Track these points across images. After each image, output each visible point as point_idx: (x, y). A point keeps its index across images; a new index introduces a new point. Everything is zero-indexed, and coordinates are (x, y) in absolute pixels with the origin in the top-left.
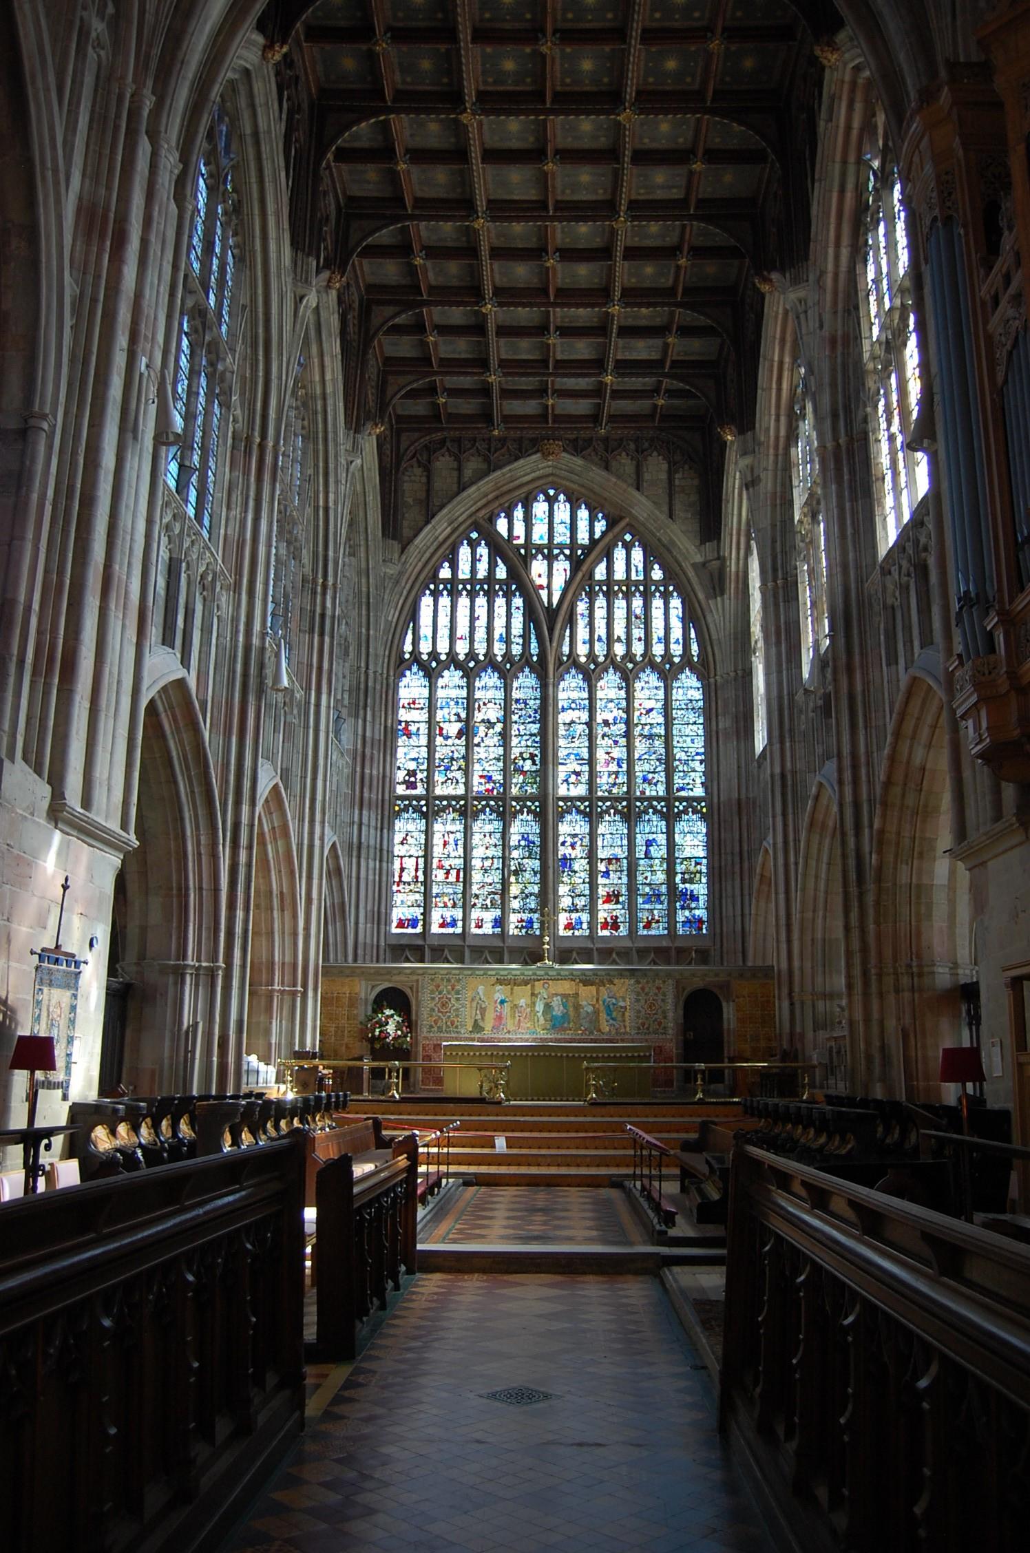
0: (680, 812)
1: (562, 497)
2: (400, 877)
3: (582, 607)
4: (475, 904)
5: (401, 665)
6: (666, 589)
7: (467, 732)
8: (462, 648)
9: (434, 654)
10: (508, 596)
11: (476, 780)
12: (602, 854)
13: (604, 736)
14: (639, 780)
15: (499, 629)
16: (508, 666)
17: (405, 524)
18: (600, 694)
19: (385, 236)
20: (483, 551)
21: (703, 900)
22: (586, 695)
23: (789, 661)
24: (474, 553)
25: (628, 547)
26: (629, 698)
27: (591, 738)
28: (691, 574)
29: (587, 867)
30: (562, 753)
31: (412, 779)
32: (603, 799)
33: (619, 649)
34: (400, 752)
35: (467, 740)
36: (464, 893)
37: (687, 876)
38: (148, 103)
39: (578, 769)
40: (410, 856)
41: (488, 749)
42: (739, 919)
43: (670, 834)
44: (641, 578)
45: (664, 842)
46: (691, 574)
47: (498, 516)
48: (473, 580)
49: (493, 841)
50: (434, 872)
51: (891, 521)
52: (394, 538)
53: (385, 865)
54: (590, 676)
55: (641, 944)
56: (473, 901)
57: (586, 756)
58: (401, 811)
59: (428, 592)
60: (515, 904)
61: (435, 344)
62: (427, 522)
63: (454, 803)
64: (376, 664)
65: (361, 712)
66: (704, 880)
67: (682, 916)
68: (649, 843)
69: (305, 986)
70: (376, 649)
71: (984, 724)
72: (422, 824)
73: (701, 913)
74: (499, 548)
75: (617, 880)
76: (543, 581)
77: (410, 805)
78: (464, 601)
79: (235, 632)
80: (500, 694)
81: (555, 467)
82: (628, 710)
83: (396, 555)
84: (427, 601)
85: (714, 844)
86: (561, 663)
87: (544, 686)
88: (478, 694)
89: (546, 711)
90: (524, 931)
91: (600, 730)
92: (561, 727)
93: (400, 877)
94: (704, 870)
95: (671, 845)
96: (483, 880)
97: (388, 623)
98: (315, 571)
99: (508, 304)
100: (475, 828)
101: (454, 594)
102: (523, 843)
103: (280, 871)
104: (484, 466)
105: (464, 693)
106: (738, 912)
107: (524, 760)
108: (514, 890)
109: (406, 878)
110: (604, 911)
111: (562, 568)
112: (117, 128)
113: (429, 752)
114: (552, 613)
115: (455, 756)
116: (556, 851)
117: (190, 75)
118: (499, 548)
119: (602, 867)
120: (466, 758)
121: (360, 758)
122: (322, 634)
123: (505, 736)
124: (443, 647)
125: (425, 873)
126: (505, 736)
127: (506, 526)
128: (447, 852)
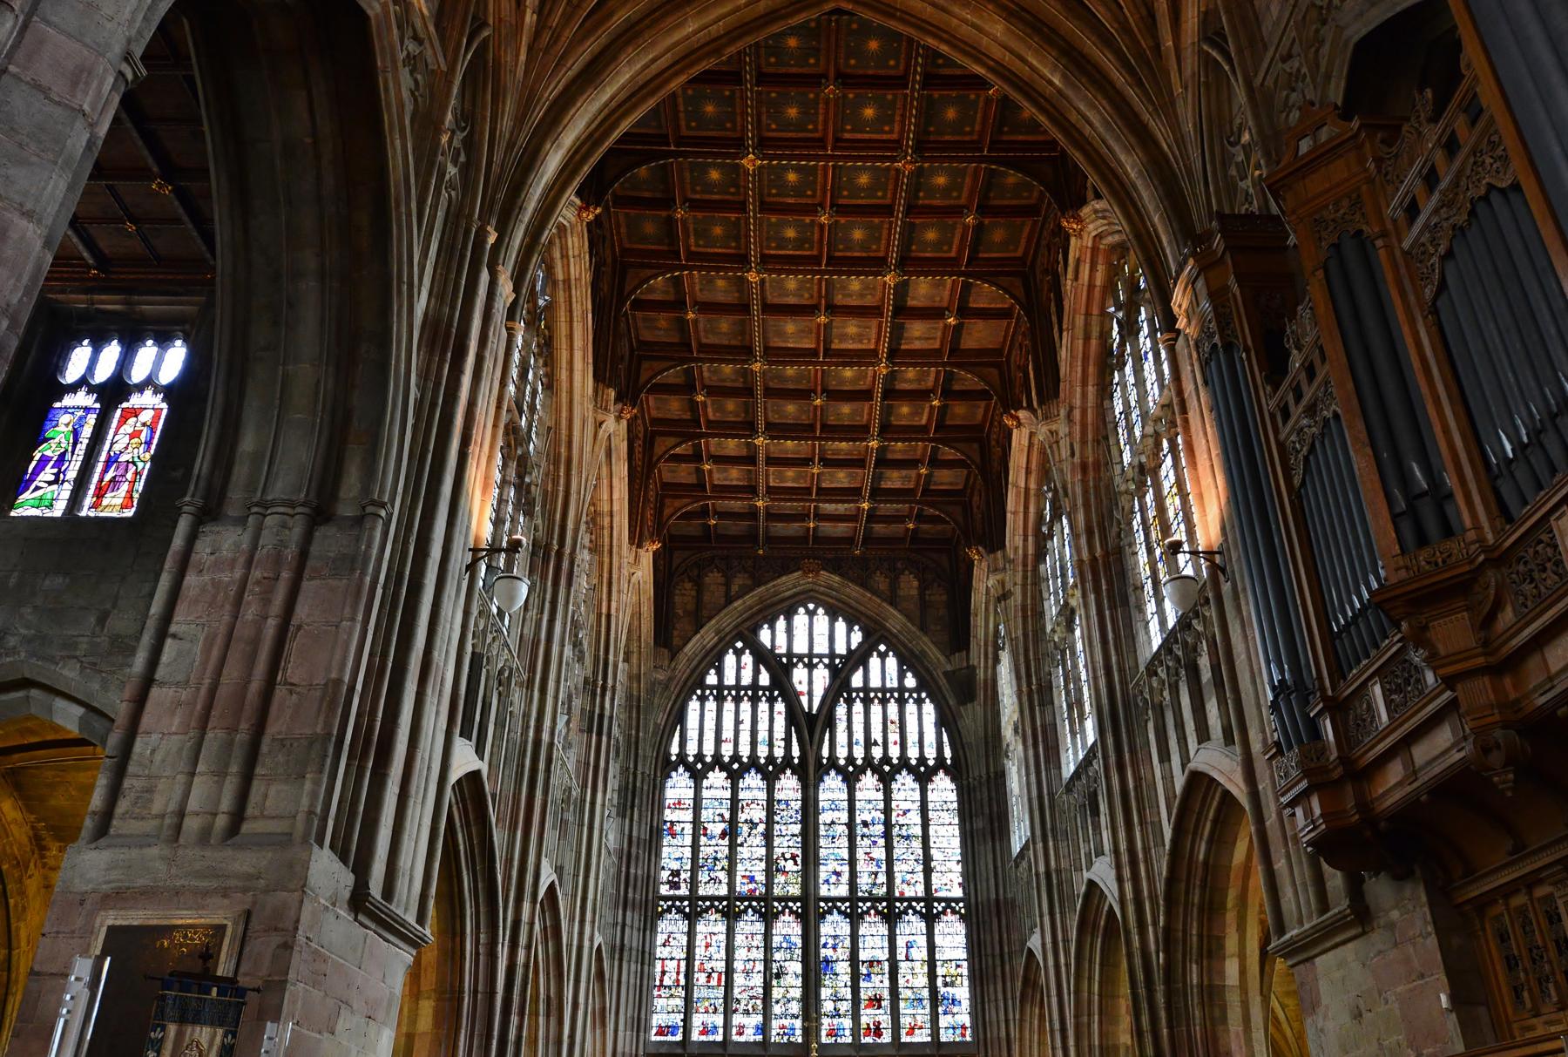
0: (939, 913)
2: (661, 981)
3: (841, 710)
4: (736, 1010)
5: (667, 767)
6: (919, 696)
7: (731, 832)
8: (727, 751)
9: (700, 757)
10: (771, 701)
11: (739, 879)
12: (863, 956)
13: (863, 836)
14: (898, 881)
15: (763, 735)
16: (771, 768)
17: (675, 633)
18: (859, 795)
19: (672, 375)
20: (747, 659)
21: (966, 1004)
22: (845, 796)
23: (1047, 762)
25: (883, 656)
26: (888, 799)
28: (943, 682)
29: (849, 970)
30: (823, 853)
31: (676, 879)
32: (864, 900)
33: (877, 753)
34: (665, 851)
35: (730, 840)
36: (725, 998)
37: (948, 979)
38: (492, 239)
39: (839, 869)
40: (672, 959)
41: (752, 849)
42: (1003, 1025)
44: (895, 684)
45: (925, 944)
46: (943, 682)
47: (761, 627)
48: (738, 687)
49: (755, 944)
50: (696, 975)
51: (1154, 626)
52: (665, 647)
53: (646, 967)
54: (851, 780)
56: (735, 1006)
57: (846, 856)
58: (664, 911)
59: (695, 697)
60: (777, 1009)
61: (710, 471)
62: (697, 632)
63: (716, 903)
64: (644, 765)
65: (628, 812)
66: (966, 983)
67: (944, 1021)
68: (909, 946)
70: (644, 750)
71: (1317, 811)
72: (683, 926)
73: (965, 1019)
74: (764, 657)
75: (877, 984)
77: (673, 906)
79: (526, 728)
80: (763, 795)
81: (814, 583)
82: (887, 811)
83: (666, 662)
84: (694, 705)
87: (805, 788)
88: (742, 795)
90: (786, 1038)
91: (860, 830)
92: (822, 827)
93: (661, 981)
94: (965, 972)
96: (748, 983)
98: (595, 673)
99: (779, 438)
100: (738, 930)
102: (784, 945)
103: (548, 974)
104: (749, 582)
105: (728, 794)
106: (1002, 1017)
107: (786, 860)
108: (776, 993)
109: (667, 982)
111: (822, 677)
112: (463, 257)
113: (693, 853)
114: (811, 718)
115: (719, 855)
116: (817, 953)
117: (526, 219)
118: (764, 657)
119: (863, 970)
120: (732, 858)
121: (626, 857)
122: (599, 734)
123: (768, 837)
124: (709, 750)
126: (768, 837)
127: (769, 637)
128: (711, 954)
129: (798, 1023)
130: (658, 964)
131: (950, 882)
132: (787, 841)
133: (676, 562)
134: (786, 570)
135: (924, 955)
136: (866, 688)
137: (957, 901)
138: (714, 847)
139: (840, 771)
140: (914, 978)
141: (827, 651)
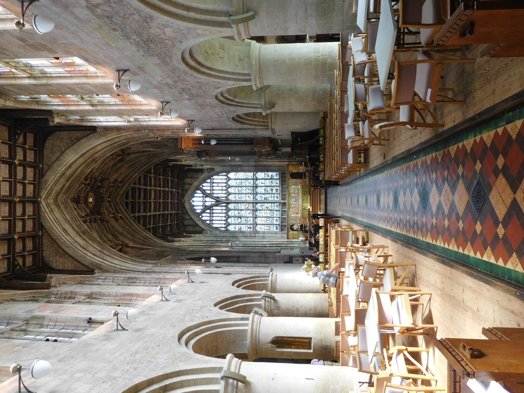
3: (215, 195)
5: (227, 230)
7: (240, 217)
9: (225, 224)
10: (213, 210)
12: (264, 192)
15: (220, 211)
17: (199, 230)
18: (233, 192)
20: (204, 215)
21: (272, 173)
25: (203, 186)
27: (242, 194)
28: (210, 174)
30: (244, 199)
33: (224, 188)
34: (244, 230)
41: (243, 213)
43: (260, 179)
46: (210, 174)
48: (210, 217)
60: (273, 208)
67: (275, 177)
68: (262, 183)
73: (275, 173)
74: (203, 211)
75: (269, 189)
78: (214, 218)
84: (214, 226)
85: (262, 171)
87: (232, 203)
88: (233, 215)
91: (240, 192)
95: (262, 179)
101: (212, 220)
105: (233, 218)
108: (270, 208)
109: (268, 228)
110: (274, 192)
111: (208, 199)
114: (217, 201)
118: (203, 211)
123: (241, 210)
124: (224, 222)
126: (241, 210)
129: (276, 204)
130: (265, 230)
131: (250, 175)
132: (243, 206)
133: (183, 230)
134: (184, 207)
135: (263, 180)
136: (210, 190)
137: (254, 174)
138: (243, 220)
139: (228, 196)
140: (268, 183)
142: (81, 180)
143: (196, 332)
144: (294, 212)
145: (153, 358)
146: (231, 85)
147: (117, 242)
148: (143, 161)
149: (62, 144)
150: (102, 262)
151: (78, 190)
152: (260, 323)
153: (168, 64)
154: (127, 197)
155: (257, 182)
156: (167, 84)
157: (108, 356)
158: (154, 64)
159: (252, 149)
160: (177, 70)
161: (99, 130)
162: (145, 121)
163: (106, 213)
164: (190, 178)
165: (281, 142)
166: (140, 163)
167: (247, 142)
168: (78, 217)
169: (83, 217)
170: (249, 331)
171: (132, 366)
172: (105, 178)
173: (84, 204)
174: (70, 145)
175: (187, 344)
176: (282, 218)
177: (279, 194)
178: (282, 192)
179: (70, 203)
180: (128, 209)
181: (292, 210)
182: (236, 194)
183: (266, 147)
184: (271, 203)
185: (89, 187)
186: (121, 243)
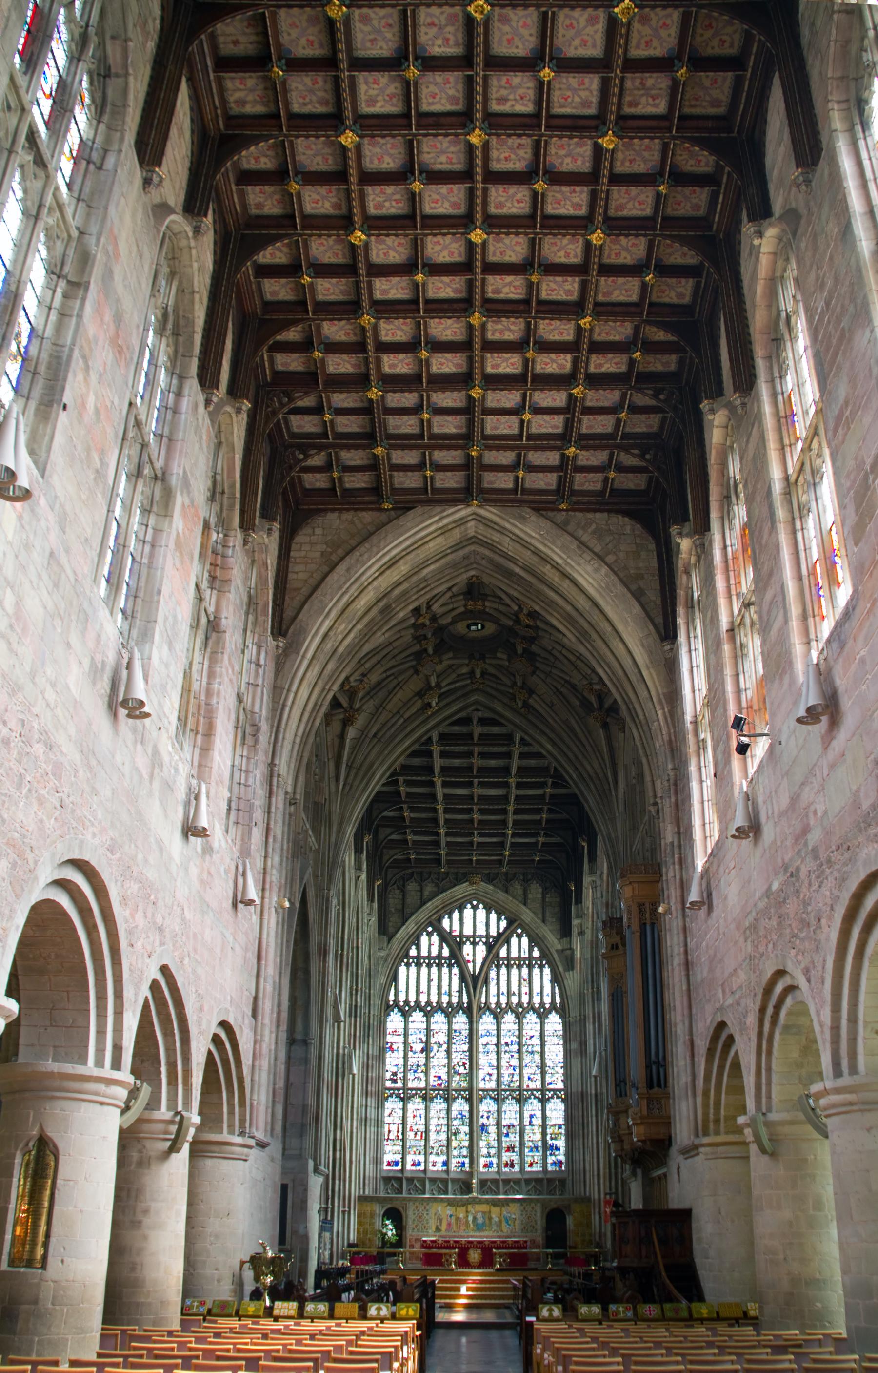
1: (481, 906)
3: (493, 974)
5: (388, 1009)
8: (423, 999)
9: (407, 1002)
10: (450, 966)
11: (432, 1078)
12: (505, 1122)
14: (526, 1079)
15: (445, 988)
18: (503, 1027)
20: (435, 938)
21: (563, 1150)
22: (495, 1027)
24: (430, 940)
25: (519, 937)
26: (520, 1029)
28: (556, 956)
32: (505, 1090)
33: (515, 1000)
36: (425, 1146)
41: (439, 1059)
46: (556, 956)
54: (498, 1017)
55: (526, 1176)
60: (455, 1153)
62: (403, 924)
67: (550, 1159)
68: (531, 1116)
69: (349, 1207)
72: (400, 1105)
73: (562, 1158)
75: (514, 1138)
76: (470, 958)
80: (446, 1027)
82: (519, 1036)
84: (402, 969)
86: (480, 1008)
87: (471, 1023)
88: (433, 1027)
89: (472, 1036)
91: (504, 1048)
94: (563, 1131)
95: (544, 1117)
96: (437, 1138)
97: (381, 985)
101: (418, 965)
104: (435, 889)
105: (424, 1025)
108: (454, 1144)
109: (392, 1136)
110: (506, 1157)
111: (481, 950)
114: (475, 978)
116: (478, 1121)
118: (445, 937)
119: (505, 1131)
122: (356, 1017)
123: (448, 1052)
124: (412, 998)
125: (403, 1134)
126: (448, 1052)
128: (416, 1123)
129: (467, 1160)
130: (386, 1127)
131: (556, 1080)
132: (459, 1057)
133: (389, 877)
134: (457, 881)
135: (540, 1122)
136: (508, 958)
137: (560, 1090)
139: (492, 1012)
140: (534, 1135)
141: (484, 933)
142: (529, 602)
143: (90, 910)
144: (441, 1221)
145: (30, 790)
146: (818, 1013)
147: (361, 695)
148: (588, 767)
149: (622, 555)
150: (303, 657)
151: (503, 596)
152: (102, 1103)
153: (860, 831)
154: (483, 721)
155: (535, 1101)
156: (806, 830)
157: (49, 672)
158: (858, 791)
159: (633, 1085)
160: (847, 855)
161: (668, 647)
162: (700, 769)
163: (439, 668)
164: (544, 898)
165: (659, 1177)
166: (580, 757)
167: (654, 1068)
168: (428, 596)
169: (429, 607)
170: (80, 1070)
171: (14, 734)
172: (538, 665)
173: (462, 609)
174: (622, 575)
175: (61, 884)
176: (422, 1181)
177: (498, 1172)
178: (507, 1182)
179: (465, 576)
180: (452, 724)
181: (449, 1212)
182: (498, 1036)
183: (642, 1129)
184: (471, 1148)
185: (511, 623)
186: (357, 706)
